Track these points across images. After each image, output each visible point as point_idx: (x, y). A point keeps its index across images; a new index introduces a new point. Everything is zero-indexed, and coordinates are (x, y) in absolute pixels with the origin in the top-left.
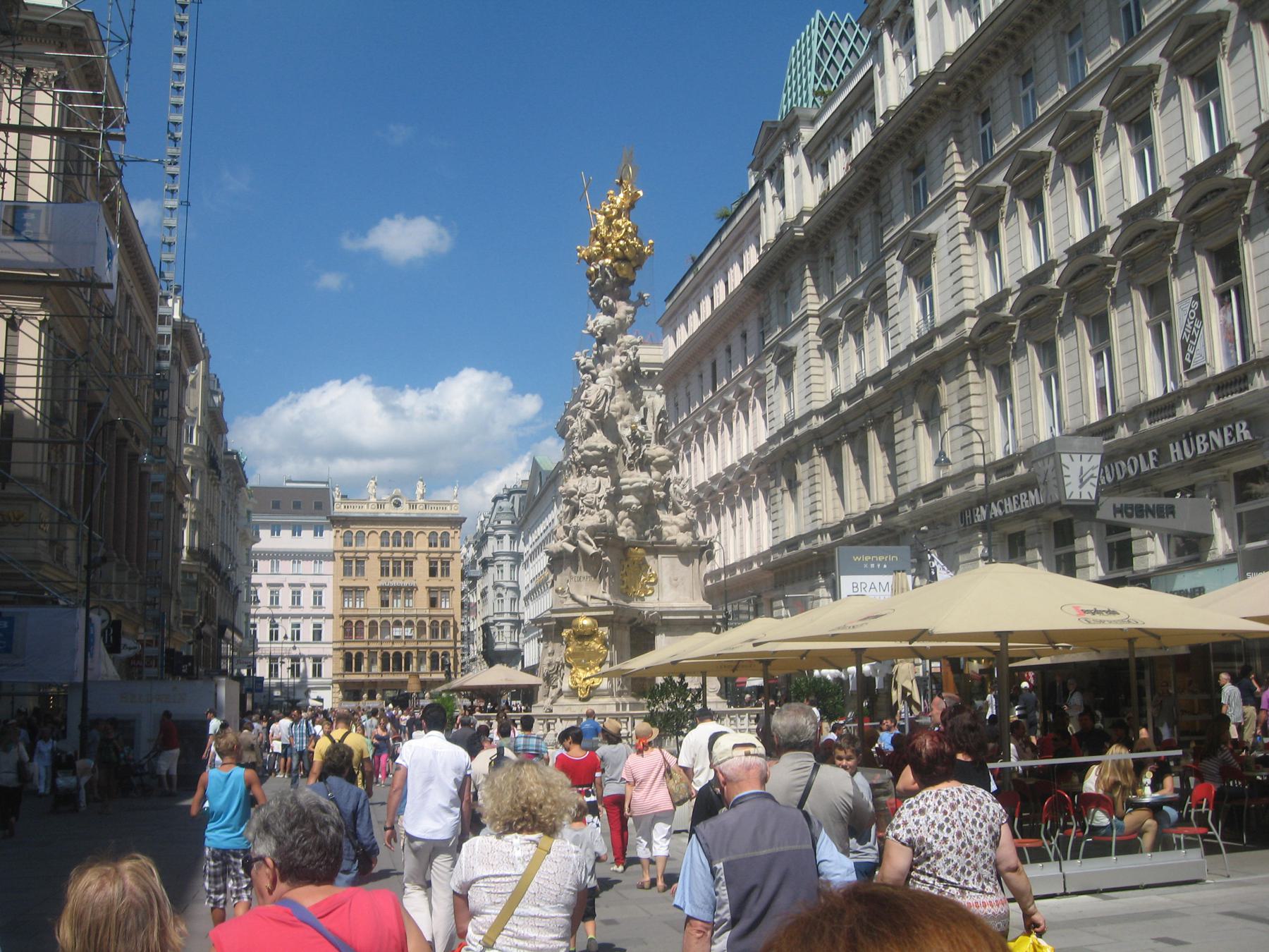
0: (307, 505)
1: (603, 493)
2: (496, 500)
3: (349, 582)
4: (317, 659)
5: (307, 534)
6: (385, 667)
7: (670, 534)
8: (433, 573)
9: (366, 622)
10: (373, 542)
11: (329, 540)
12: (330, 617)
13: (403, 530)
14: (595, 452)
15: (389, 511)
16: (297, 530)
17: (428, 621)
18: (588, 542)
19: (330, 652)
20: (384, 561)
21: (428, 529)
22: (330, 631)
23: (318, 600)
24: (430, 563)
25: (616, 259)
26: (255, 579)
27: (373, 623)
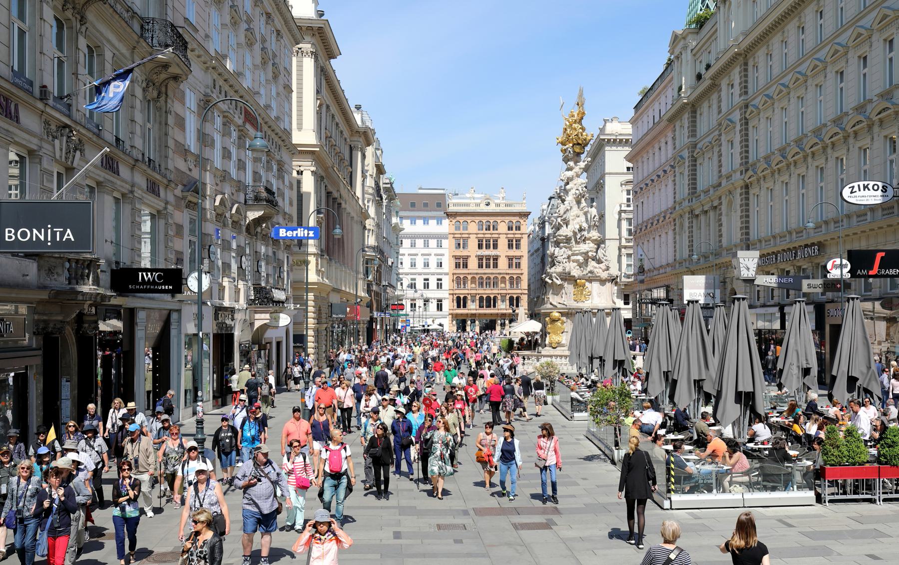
0: (433, 204)
1: (565, 256)
2: (550, 199)
3: (459, 253)
5: (433, 222)
6: (481, 306)
8: (510, 246)
9: (469, 277)
11: (446, 226)
12: (447, 274)
13: (492, 219)
15: (484, 208)
16: (426, 220)
17: (507, 277)
19: (447, 296)
21: (507, 219)
22: (447, 282)
26: (401, 251)
27: (473, 278)
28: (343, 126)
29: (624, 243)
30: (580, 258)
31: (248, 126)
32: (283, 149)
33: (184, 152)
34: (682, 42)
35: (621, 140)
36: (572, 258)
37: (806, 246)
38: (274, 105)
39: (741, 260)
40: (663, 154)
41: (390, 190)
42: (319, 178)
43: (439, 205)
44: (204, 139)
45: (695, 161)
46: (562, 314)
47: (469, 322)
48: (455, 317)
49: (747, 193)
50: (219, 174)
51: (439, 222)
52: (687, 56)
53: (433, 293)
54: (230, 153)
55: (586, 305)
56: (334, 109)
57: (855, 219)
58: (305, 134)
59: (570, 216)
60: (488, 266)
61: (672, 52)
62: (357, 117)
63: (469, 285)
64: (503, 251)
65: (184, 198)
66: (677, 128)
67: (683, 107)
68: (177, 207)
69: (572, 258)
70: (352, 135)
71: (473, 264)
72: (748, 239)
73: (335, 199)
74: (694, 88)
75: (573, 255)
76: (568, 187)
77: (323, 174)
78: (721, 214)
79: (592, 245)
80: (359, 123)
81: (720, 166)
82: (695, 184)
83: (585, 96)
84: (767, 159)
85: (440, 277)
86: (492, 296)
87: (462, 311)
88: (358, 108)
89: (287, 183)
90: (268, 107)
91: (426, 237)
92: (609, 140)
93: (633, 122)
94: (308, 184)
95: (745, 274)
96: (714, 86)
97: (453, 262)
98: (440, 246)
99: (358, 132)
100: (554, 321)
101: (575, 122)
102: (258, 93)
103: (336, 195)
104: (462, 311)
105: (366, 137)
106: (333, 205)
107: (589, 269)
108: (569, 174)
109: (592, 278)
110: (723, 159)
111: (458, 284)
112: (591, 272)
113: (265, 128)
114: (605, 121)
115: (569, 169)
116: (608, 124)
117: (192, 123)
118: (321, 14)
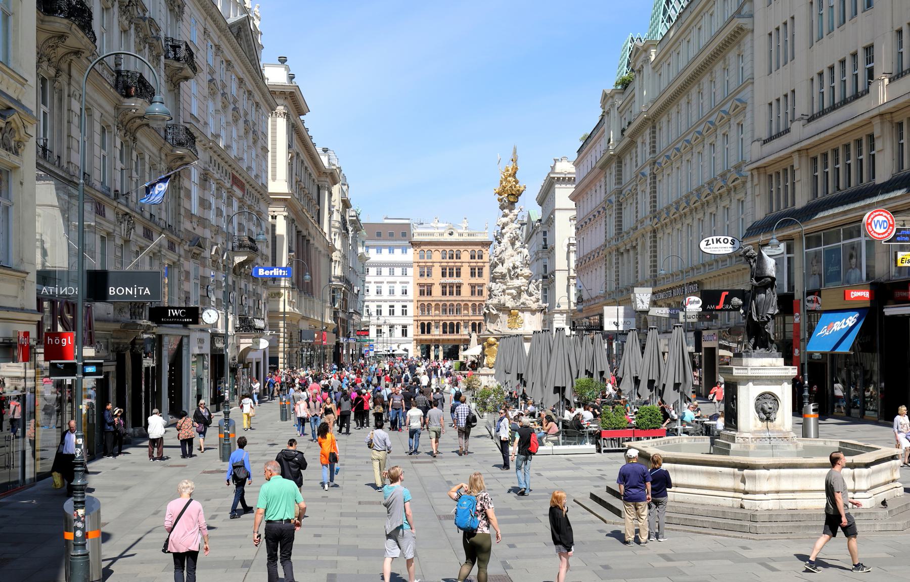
0: (399, 234)
4: (404, 327)
5: (398, 251)
6: (445, 332)
8: (473, 274)
9: (433, 304)
11: (411, 255)
12: (411, 301)
13: (455, 249)
15: (447, 238)
16: (391, 249)
17: (470, 304)
21: (470, 248)
22: (411, 309)
23: (405, 292)
26: (367, 279)
27: (437, 305)
28: (311, 169)
29: (572, 273)
30: (514, 292)
31: (235, 188)
32: (261, 201)
33: (191, 216)
34: (610, 100)
36: (507, 291)
37: (691, 284)
38: (254, 166)
39: (637, 295)
40: (597, 198)
41: (356, 223)
42: (290, 221)
43: (404, 234)
44: (203, 203)
45: (621, 205)
46: (498, 339)
47: (433, 348)
48: (419, 342)
49: (655, 237)
50: (213, 229)
51: (404, 251)
52: (614, 113)
53: (398, 320)
54: (222, 211)
55: (520, 331)
56: (303, 156)
57: (734, 259)
58: (278, 183)
59: (505, 255)
60: (451, 293)
61: (603, 107)
62: (324, 160)
63: (433, 312)
64: (465, 279)
65: (190, 251)
66: (608, 175)
67: (611, 158)
68: (186, 259)
69: (507, 291)
70: (319, 176)
71: (437, 291)
72: (656, 276)
73: (304, 237)
74: (619, 141)
75: (508, 289)
76: (504, 231)
77: (294, 217)
78: (637, 254)
79: (524, 280)
80: (326, 164)
81: (637, 212)
82: (621, 225)
83: (518, 153)
84: (668, 208)
85: (404, 304)
86: (455, 323)
87: (426, 337)
88: (325, 150)
89: (264, 229)
90: (249, 168)
91: (392, 266)
92: (559, 178)
93: (577, 164)
94: (281, 228)
95: (641, 306)
96: (632, 143)
97: (418, 289)
98: (405, 274)
99: (325, 173)
100: (490, 345)
101: (510, 176)
102: (242, 159)
103: (305, 233)
104: (426, 337)
105: (333, 177)
106: (303, 242)
107: (521, 301)
108: (505, 220)
109: (524, 309)
110: (639, 206)
111: (423, 310)
112: (523, 303)
113: (247, 186)
114: (556, 161)
115: (505, 216)
116: (557, 163)
117: (195, 193)
118: (291, 77)
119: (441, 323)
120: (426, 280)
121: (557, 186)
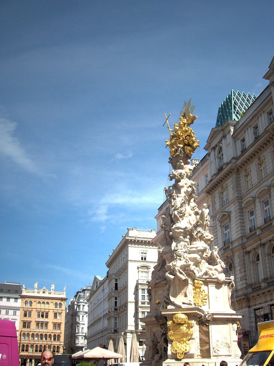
3: (26, 319)
5: (12, 300)
6: (36, 351)
7: (213, 275)
10: (35, 305)
11: (19, 303)
13: (46, 301)
14: (180, 230)
15: (41, 295)
17: (53, 335)
18: (181, 273)
20: (39, 312)
21: (55, 301)
24: (55, 314)
25: (185, 145)
27: (33, 334)
35: (138, 241)
47: (28, 360)
64: (51, 319)
71: (33, 326)
92: (131, 240)
97: (22, 324)
98: (15, 314)
114: (128, 230)
116: (130, 232)
119: (35, 345)
120: (27, 319)
121: (129, 245)
